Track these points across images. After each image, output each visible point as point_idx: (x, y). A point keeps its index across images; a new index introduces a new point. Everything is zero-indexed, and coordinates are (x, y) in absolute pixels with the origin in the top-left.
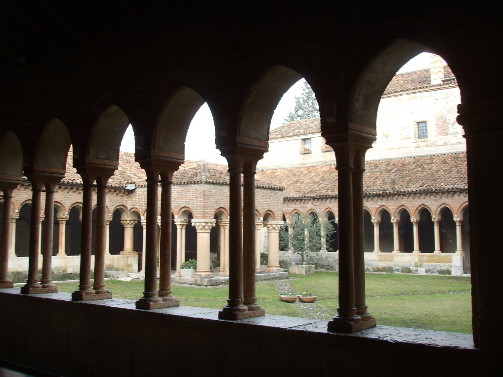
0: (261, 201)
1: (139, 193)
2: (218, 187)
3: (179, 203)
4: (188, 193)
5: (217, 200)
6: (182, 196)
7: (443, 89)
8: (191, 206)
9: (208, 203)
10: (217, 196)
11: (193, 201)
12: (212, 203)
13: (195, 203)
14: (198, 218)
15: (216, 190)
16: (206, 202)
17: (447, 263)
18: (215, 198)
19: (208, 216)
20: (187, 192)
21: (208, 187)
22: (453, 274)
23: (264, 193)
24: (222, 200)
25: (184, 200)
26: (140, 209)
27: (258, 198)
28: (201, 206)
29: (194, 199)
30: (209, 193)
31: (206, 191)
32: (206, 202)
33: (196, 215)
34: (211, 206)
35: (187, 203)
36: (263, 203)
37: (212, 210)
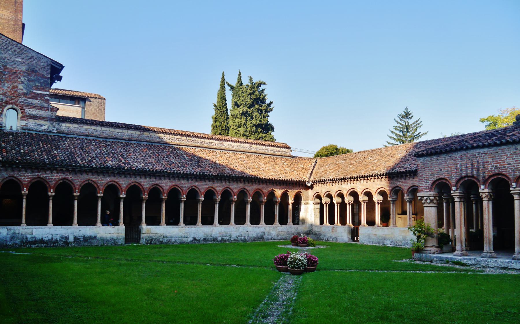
0: (511, 160)
2: (434, 158)
5: (435, 171)
9: (423, 176)
10: (435, 167)
12: (427, 176)
15: (433, 161)
16: (421, 176)
18: (431, 170)
19: (423, 190)
21: (421, 160)
23: (515, 149)
24: (441, 170)
27: (504, 158)
30: (424, 166)
31: (419, 164)
32: (421, 176)
34: (427, 179)
36: (515, 164)
37: (428, 183)
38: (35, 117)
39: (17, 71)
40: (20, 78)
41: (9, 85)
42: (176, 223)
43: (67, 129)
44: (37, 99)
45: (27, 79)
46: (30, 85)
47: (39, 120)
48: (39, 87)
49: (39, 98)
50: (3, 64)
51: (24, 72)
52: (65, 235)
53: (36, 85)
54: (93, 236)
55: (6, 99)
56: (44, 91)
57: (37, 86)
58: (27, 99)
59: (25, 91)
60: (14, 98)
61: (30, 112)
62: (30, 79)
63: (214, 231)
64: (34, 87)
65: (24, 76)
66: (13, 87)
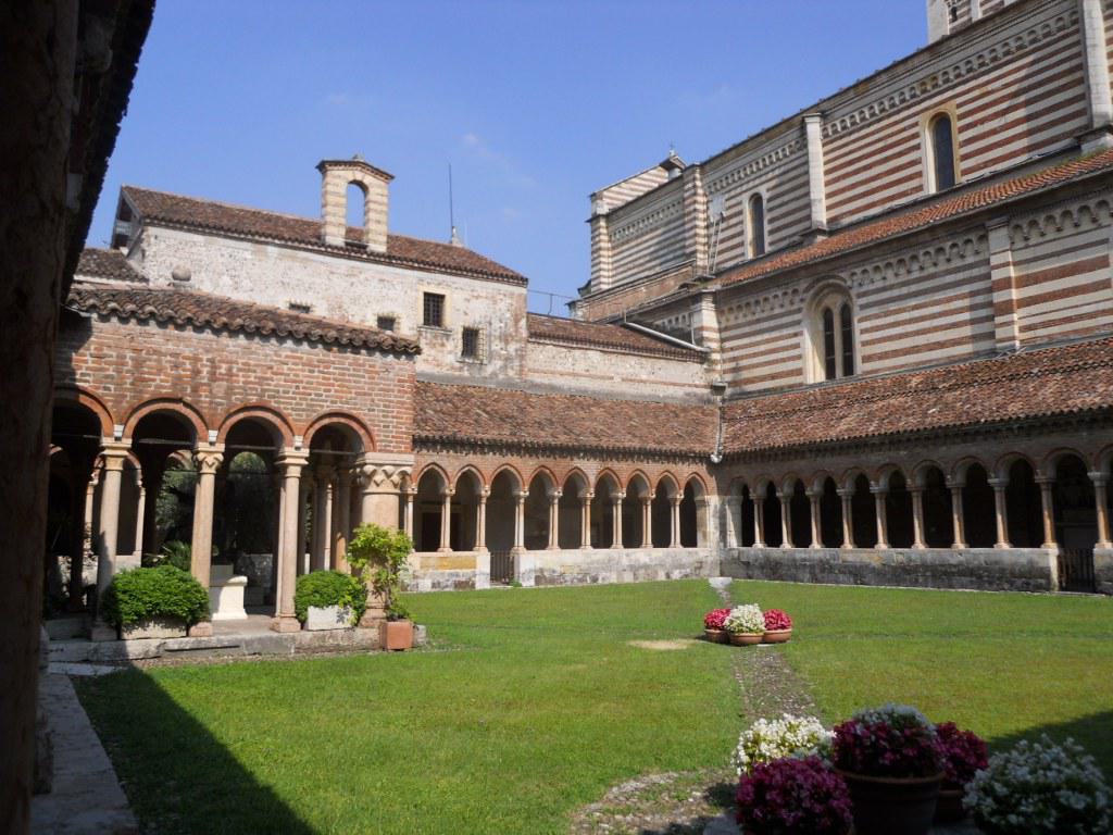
1: (106, 338)
3: (312, 400)
4: (351, 372)
6: (324, 378)
7: (349, 258)
8: (365, 415)
11: (373, 400)
13: (378, 406)
14: (392, 452)
17: (467, 567)
20: (348, 370)
22: (478, 586)
25: (336, 391)
26: (107, 395)
28: (402, 418)
29: (377, 395)
33: (382, 441)
35: (347, 403)
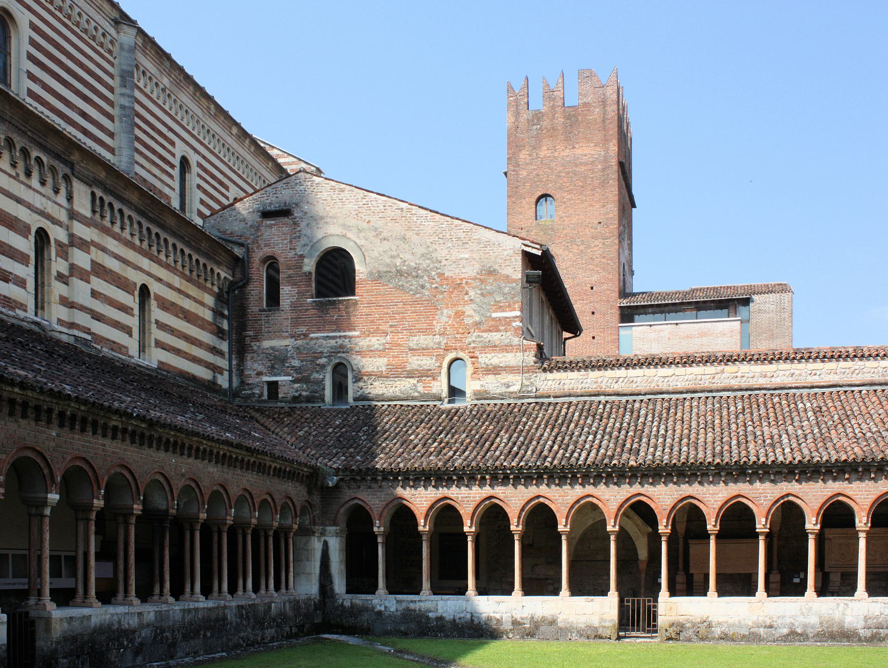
38: (495, 370)
39: (461, 280)
40: (467, 294)
41: (450, 312)
42: (847, 588)
43: (557, 386)
44: (498, 331)
45: (479, 292)
46: (485, 303)
47: (504, 374)
48: (501, 305)
49: (502, 328)
50: (439, 271)
51: (474, 279)
52: (495, 615)
53: (495, 301)
54: (550, 618)
55: (445, 341)
56: (511, 311)
57: (499, 302)
58: (481, 334)
59: (477, 318)
60: (459, 336)
61: (487, 361)
62: (484, 292)
63: (848, 612)
64: (493, 305)
65: (474, 288)
66: (456, 313)
